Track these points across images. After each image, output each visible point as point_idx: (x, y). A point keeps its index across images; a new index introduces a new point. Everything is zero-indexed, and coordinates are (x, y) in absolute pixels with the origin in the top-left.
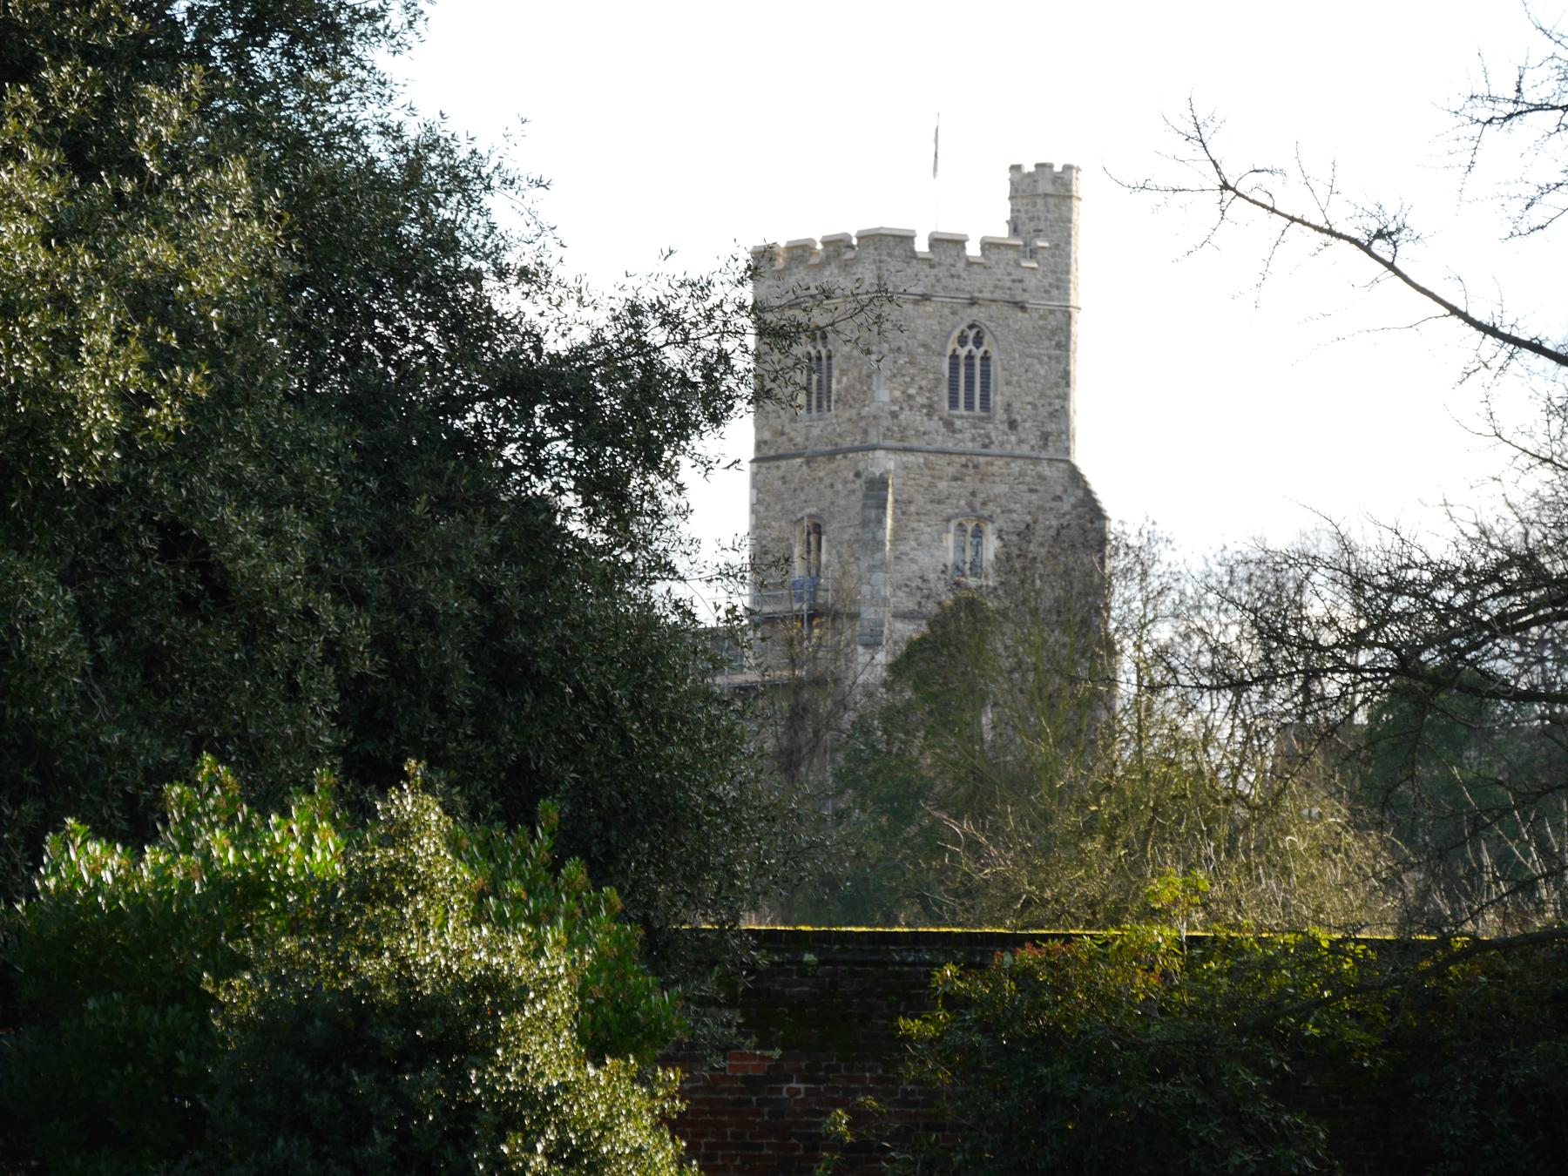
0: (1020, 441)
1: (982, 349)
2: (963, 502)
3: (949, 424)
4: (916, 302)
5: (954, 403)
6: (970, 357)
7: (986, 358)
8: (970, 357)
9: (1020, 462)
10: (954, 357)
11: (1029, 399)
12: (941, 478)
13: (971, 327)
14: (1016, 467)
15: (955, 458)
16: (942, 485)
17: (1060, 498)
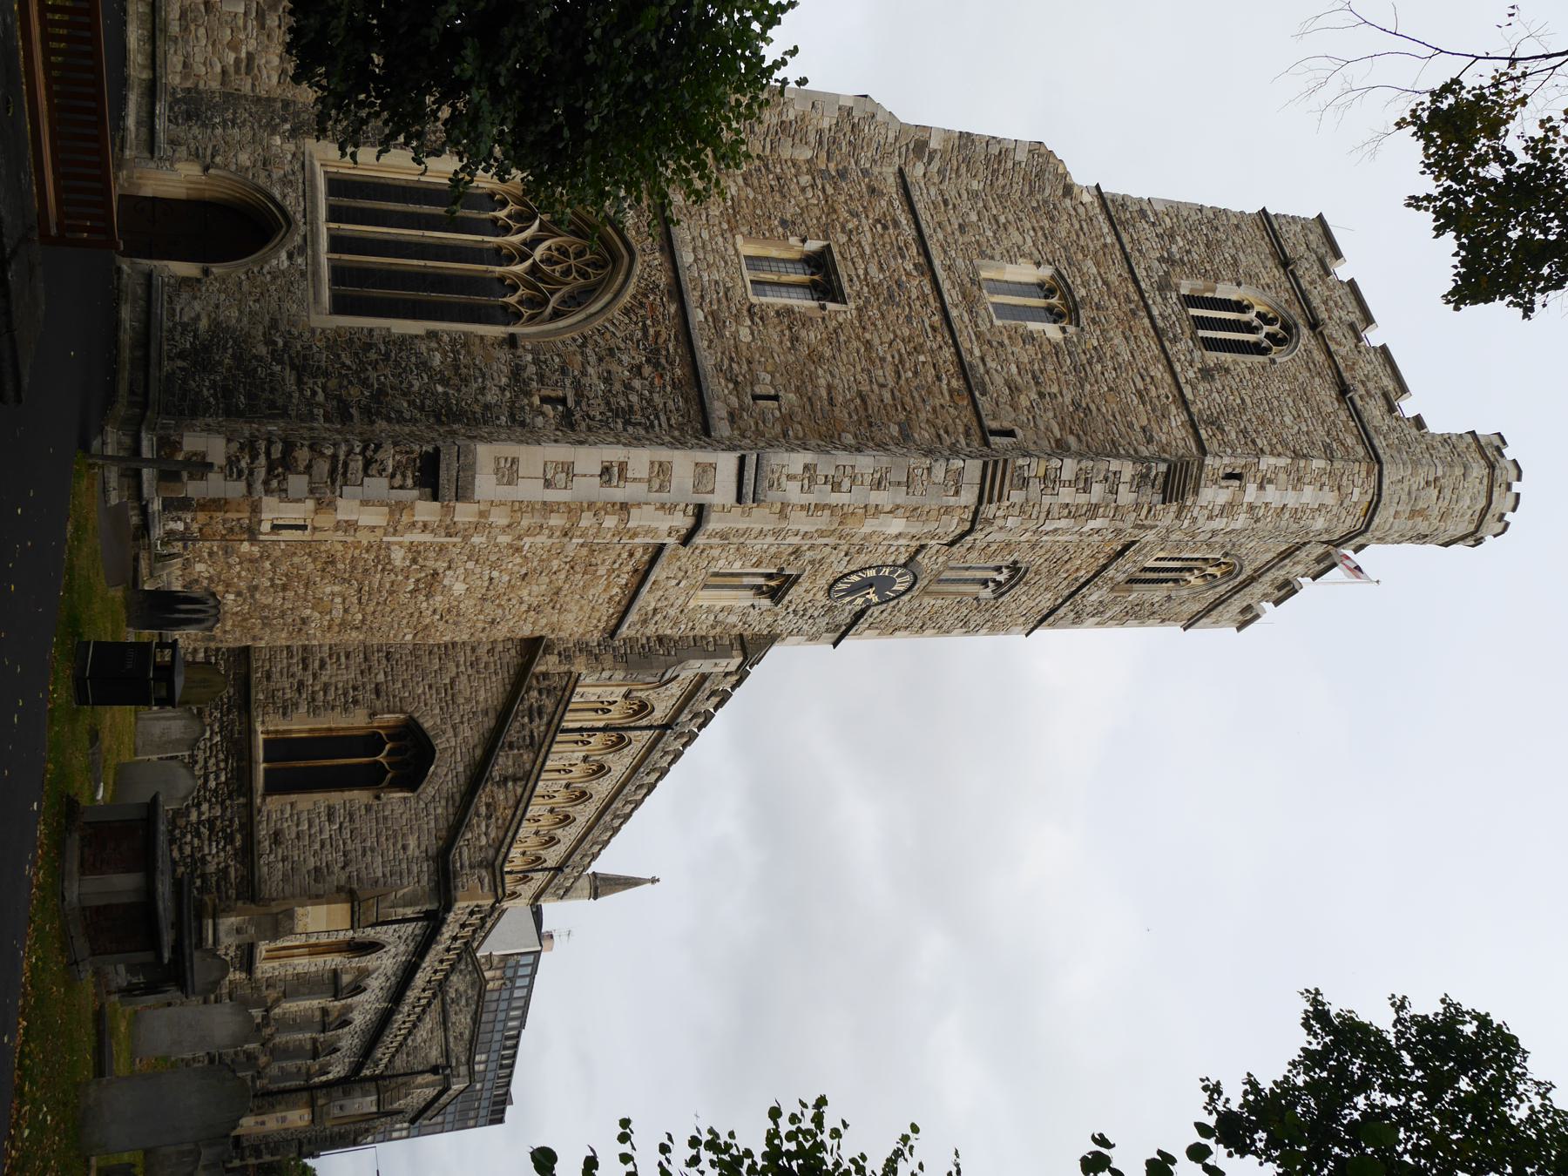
0: (1194, 388)
1: (1266, 343)
2: (1083, 292)
3: (1164, 286)
4: (1274, 255)
5: (1191, 301)
6: (1249, 328)
7: (1256, 349)
8: (1249, 328)
9: (1168, 377)
10: (1240, 307)
11: (1248, 400)
12: (1097, 264)
13: (1285, 327)
14: (1158, 371)
15: (1131, 288)
16: (1090, 267)
17: (1150, 440)
